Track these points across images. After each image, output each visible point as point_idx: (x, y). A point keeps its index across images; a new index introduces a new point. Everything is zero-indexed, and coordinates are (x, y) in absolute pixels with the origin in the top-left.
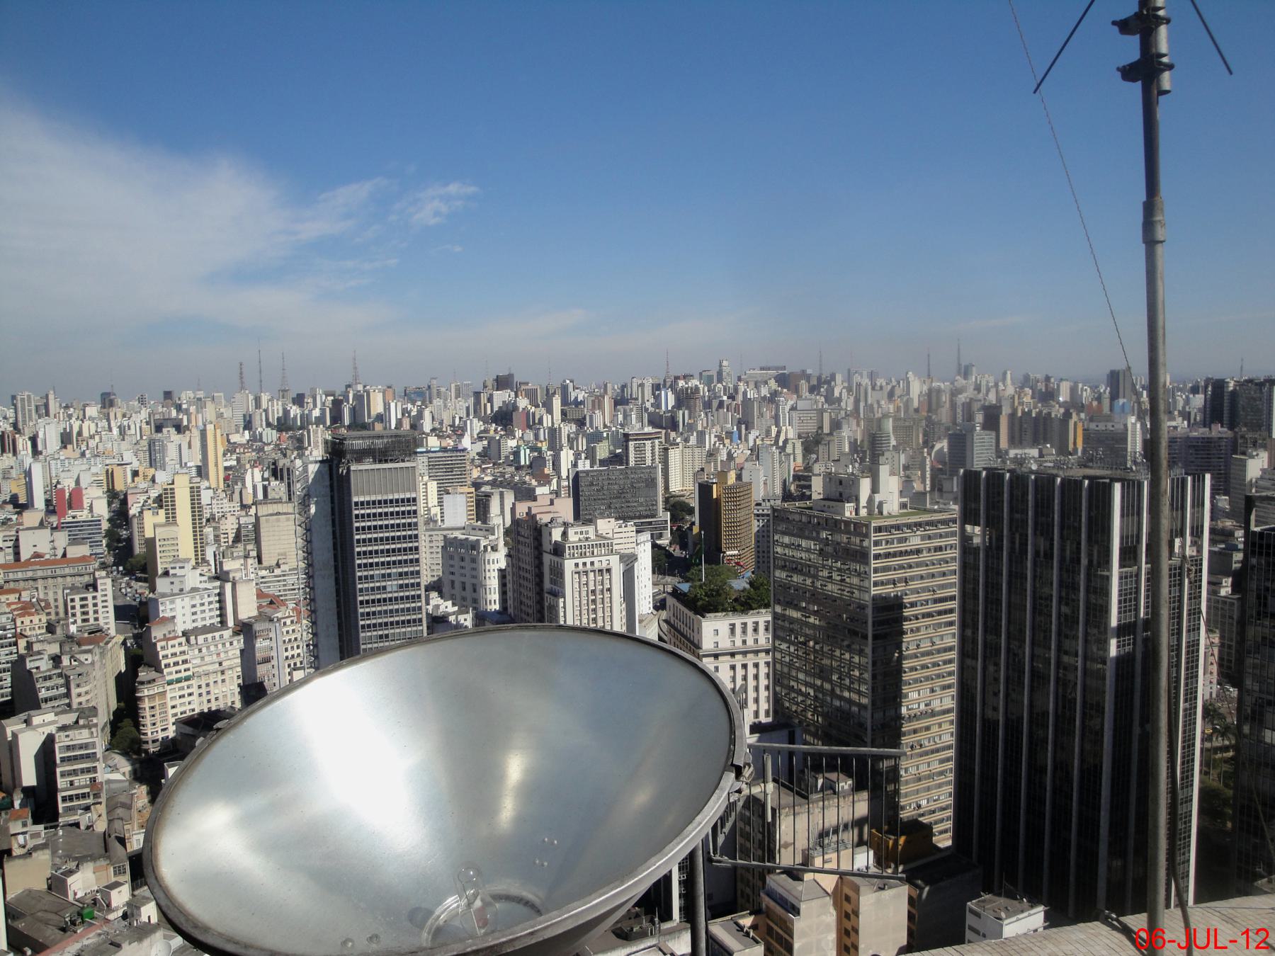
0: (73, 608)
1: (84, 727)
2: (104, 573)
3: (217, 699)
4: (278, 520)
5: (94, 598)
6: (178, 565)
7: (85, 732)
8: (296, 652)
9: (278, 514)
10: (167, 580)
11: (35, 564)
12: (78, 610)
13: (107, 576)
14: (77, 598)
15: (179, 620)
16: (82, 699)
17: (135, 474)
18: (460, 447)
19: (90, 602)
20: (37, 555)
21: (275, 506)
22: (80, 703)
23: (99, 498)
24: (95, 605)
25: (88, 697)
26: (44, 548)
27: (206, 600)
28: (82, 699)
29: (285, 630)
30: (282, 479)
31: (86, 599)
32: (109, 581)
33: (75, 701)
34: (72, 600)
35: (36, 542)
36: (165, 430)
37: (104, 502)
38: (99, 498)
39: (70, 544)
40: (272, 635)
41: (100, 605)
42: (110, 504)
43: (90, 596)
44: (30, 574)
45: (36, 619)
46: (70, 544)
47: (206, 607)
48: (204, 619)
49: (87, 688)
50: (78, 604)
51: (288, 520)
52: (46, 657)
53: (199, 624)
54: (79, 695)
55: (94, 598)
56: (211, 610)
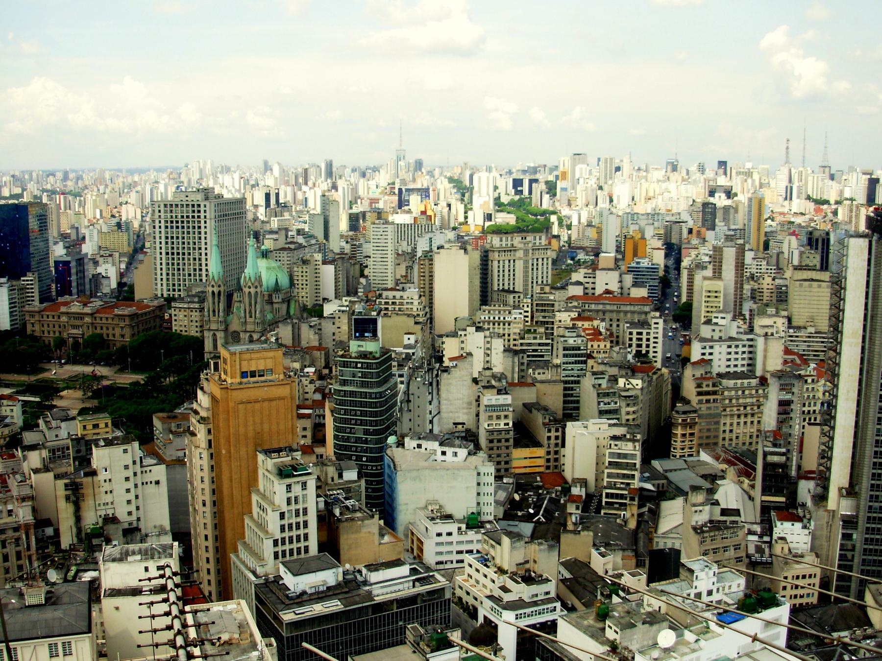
0: (631, 339)
1: (629, 440)
2: (657, 314)
3: (737, 437)
4: (810, 286)
5: (648, 334)
7: (630, 445)
8: (812, 409)
9: (812, 280)
10: (710, 327)
11: (606, 298)
12: (634, 342)
13: (660, 317)
14: (635, 331)
15: (715, 363)
16: (630, 417)
17: (690, 231)
19: (644, 337)
20: (607, 292)
21: (809, 272)
22: (628, 420)
23: (659, 249)
24: (648, 340)
25: (634, 416)
26: (614, 287)
27: (740, 349)
28: (630, 417)
29: (806, 386)
30: (817, 249)
31: (641, 334)
32: (661, 321)
33: (624, 417)
34: (631, 333)
35: (606, 281)
36: (717, 195)
37: (662, 253)
38: (659, 249)
39: (633, 286)
40: (795, 390)
41: (652, 340)
42: (667, 256)
43: (645, 332)
44: (600, 307)
45: (602, 344)
46: (633, 286)
47: (739, 356)
48: (736, 366)
49: (634, 409)
50: (635, 336)
51: (819, 286)
52: (607, 377)
53: (732, 370)
54: (628, 413)
55: (648, 334)
56: (743, 359)
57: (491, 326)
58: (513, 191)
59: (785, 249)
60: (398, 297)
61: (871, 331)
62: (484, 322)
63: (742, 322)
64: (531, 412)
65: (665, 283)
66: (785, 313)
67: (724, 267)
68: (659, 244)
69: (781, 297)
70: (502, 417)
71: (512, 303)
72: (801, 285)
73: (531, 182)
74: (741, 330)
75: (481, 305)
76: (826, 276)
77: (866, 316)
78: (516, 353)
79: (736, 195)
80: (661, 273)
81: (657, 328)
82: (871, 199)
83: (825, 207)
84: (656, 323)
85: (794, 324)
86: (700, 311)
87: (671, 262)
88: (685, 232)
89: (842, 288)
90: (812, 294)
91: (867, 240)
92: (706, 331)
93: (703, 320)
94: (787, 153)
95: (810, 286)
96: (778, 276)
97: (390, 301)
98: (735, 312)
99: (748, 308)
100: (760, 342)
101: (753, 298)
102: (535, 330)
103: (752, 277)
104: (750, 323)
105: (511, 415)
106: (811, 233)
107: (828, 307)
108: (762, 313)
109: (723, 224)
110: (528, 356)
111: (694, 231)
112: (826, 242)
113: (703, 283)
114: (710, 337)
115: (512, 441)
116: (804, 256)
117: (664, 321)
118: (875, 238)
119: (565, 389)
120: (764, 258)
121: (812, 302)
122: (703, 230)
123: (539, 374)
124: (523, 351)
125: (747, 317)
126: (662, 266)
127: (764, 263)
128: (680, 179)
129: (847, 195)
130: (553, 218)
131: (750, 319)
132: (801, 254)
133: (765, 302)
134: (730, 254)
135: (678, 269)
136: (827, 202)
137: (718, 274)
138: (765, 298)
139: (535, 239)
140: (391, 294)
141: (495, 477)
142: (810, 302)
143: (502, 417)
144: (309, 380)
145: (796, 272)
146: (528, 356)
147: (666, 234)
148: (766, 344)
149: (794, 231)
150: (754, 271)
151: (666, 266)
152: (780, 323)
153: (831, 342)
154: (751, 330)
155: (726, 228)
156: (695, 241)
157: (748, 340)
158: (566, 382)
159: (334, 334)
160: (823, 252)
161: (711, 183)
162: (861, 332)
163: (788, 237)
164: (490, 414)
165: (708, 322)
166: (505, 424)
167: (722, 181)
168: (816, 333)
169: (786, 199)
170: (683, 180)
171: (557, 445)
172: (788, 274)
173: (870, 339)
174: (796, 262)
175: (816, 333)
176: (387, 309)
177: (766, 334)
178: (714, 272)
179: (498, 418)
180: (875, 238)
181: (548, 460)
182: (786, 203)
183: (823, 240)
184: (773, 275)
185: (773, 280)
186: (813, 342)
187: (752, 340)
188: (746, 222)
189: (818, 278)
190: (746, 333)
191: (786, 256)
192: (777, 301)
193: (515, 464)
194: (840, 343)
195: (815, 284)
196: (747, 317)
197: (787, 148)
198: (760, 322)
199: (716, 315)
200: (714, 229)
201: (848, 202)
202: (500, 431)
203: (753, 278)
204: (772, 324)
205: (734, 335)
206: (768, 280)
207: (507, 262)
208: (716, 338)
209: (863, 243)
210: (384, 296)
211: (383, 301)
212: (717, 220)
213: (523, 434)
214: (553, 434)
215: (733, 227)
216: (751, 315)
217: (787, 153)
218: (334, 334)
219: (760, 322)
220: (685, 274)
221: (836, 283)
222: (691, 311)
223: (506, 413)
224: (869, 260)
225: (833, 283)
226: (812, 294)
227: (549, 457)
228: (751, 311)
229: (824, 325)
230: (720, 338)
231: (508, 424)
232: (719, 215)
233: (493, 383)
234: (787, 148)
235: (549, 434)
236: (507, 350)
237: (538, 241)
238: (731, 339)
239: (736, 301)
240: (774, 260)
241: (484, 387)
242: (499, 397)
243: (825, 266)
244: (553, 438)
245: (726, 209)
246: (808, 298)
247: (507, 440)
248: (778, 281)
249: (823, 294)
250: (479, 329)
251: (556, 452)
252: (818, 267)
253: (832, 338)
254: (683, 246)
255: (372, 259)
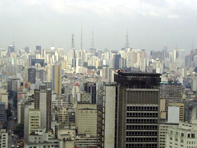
2: (5, 130)
4: (87, 112)
6: (39, 130)
9: (87, 109)
10: (33, 137)
17: (22, 84)
18: (178, 83)
21: (86, 105)
23: (5, 94)
30: (89, 92)
32: (7, 134)
36: (36, 64)
37: (7, 96)
38: (5, 94)
42: (9, 98)
51: (92, 112)
59: (73, 93)
61: (119, 135)
63: (51, 133)
65: (9, 114)
66: (74, 127)
67: (40, 103)
68: (5, 91)
69: (72, 119)
72: (82, 112)
74: (51, 137)
76: (95, 107)
77: (116, 127)
79: (46, 64)
80: (6, 107)
81: (4, 138)
82: (116, 65)
83: (93, 70)
84: (4, 135)
85: (79, 133)
86: (29, 128)
87: (12, 102)
88: (19, 84)
89: (103, 113)
90: (88, 116)
91: (115, 87)
92: (31, 139)
93: (30, 132)
94: (73, 42)
95: (87, 112)
96: (70, 107)
98: (47, 127)
99: (54, 125)
100: (61, 143)
101: (57, 120)
103: (56, 108)
104: (55, 133)
106: (86, 84)
107: (97, 123)
108: (62, 127)
109: (39, 80)
111: (24, 84)
112: (94, 88)
113: (30, 111)
114: (34, 142)
116: (83, 96)
117: (9, 134)
118: (119, 86)
120: (62, 98)
121: (88, 121)
122: (29, 83)
125: (54, 130)
126: (7, 104)
127: (62, 100)
128: (16, 56)
129: (104, 64)
131: (55, 131)
132: (81, 95)
133: (63, 121)
134: (43, 96)
135: (16, 105)
136: (94, 67)
137: (37, 107)
138: (63, 120)
142: (87, 122)
145: (79, 105)
147: (8, 86)
148: (64, 144)
149: (78, 83)
150: (57, 105)
151: (9, 104)
152: (72, 133)
153: (99, 142)
154: (56, 137)
155: (41, 82)
156: (24, 90)
157: (55, 143)
160: (93, 94)
161: (33, 58)
162: (114, 136)
163: (74, 87)
165: (33, 134)
167: (39, 57)
168: (91, 137)
169: (73, 66)
170: (18, 56)
172: (75, 106)
173: (119, 139)
174: (79, 100)
175: (91, 137)
177: (64, 139)
178: (35, 106)
180: (119, 86)
182: (73, 68)
183: (93, 88)
184: (67, 107)
185: (67, 109)
186: (89, 142)
187: (57, 142)
188: (52, 79)
189: (91, 108)
190: (53, 139)
191: (74, 96)
192: (70, 121)
194: (104, 142)
195: (89, 111)
196: (54, 130)
197: (73, 39)
198: (61, 133)
199: (37, 130)
200: (35, 83)
201: (105, 67)
203: (56, 109)
204: (67, 133)
205: (48, 141)
206: (65, 110)
208: (37, 142)
209: (113, 89)
212: (36, 78)
215: (45, 82)
216: (55, 129)
217: (73, 42)
219: (61, 133)
220: (19, 108)
221: (100, 110)
222: (23, 128)
224: (116, 98)
225: (98, 110)
226: (88, 116)
228: (56, 127)
229: (94, 133)
230: (40, 142)
232: (37, 74)
234: (73, 39)
238: (45, 142)
239: (47, 122)
240: (67, 99)
243: (94, 102)
245: (41, 72)
246: (86, 119)
248: (70, 111)
249: (93, 116)
252: (91, 102)
253: (99, 140)
254: (18, 92)
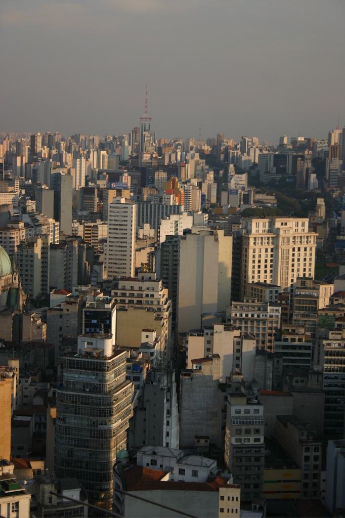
57: (243, 325)
58: (274, 169)
60: (136, 288)
62: (235, 320)
64: (286, 426)
70: (252, 432)
71: (268, 299)
73: (295, 158)
75: (232, 299)
78: (270, 356)
97: (128, 293)
102: (294, 331)
105: (262, 428)
110: (285, 360)
115: (263, 460)
119: (327, 401)
123: (297, 382)
124: (278, 355)
130: (320, 201)
139: (297, 225)
140: (128, 284)
141: (242, 503)
143: (252, 432)
144: (27, 254)
146: (285, 360)
158: (328, 393)
159: (61, 329)
164: (239, 427)
166: (257, 440)
171: (316, 467)
176: (123, 302)
179: (248, 432)
181: (306, 485)
193: (266, 487)
202: (249, 448)
207: (263, 251)
210: (120, 286)
211: (119, 292)
213: (277, 451)
214: (312, 454)
218: (61, 329)
223: (257, 427)
227: (307, 481)
231: (258, 440)
233: (243, 390)
235: (307, 454)
236: (259, 352)
237: (300, 228)
241: (232, 395)
242: (249, 407)
244: (312, 459)
247: (257, 459)
250: (228, 328)
251: (316, 476)
255: (108, 244)
